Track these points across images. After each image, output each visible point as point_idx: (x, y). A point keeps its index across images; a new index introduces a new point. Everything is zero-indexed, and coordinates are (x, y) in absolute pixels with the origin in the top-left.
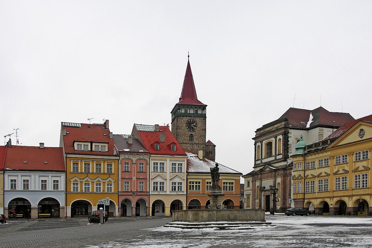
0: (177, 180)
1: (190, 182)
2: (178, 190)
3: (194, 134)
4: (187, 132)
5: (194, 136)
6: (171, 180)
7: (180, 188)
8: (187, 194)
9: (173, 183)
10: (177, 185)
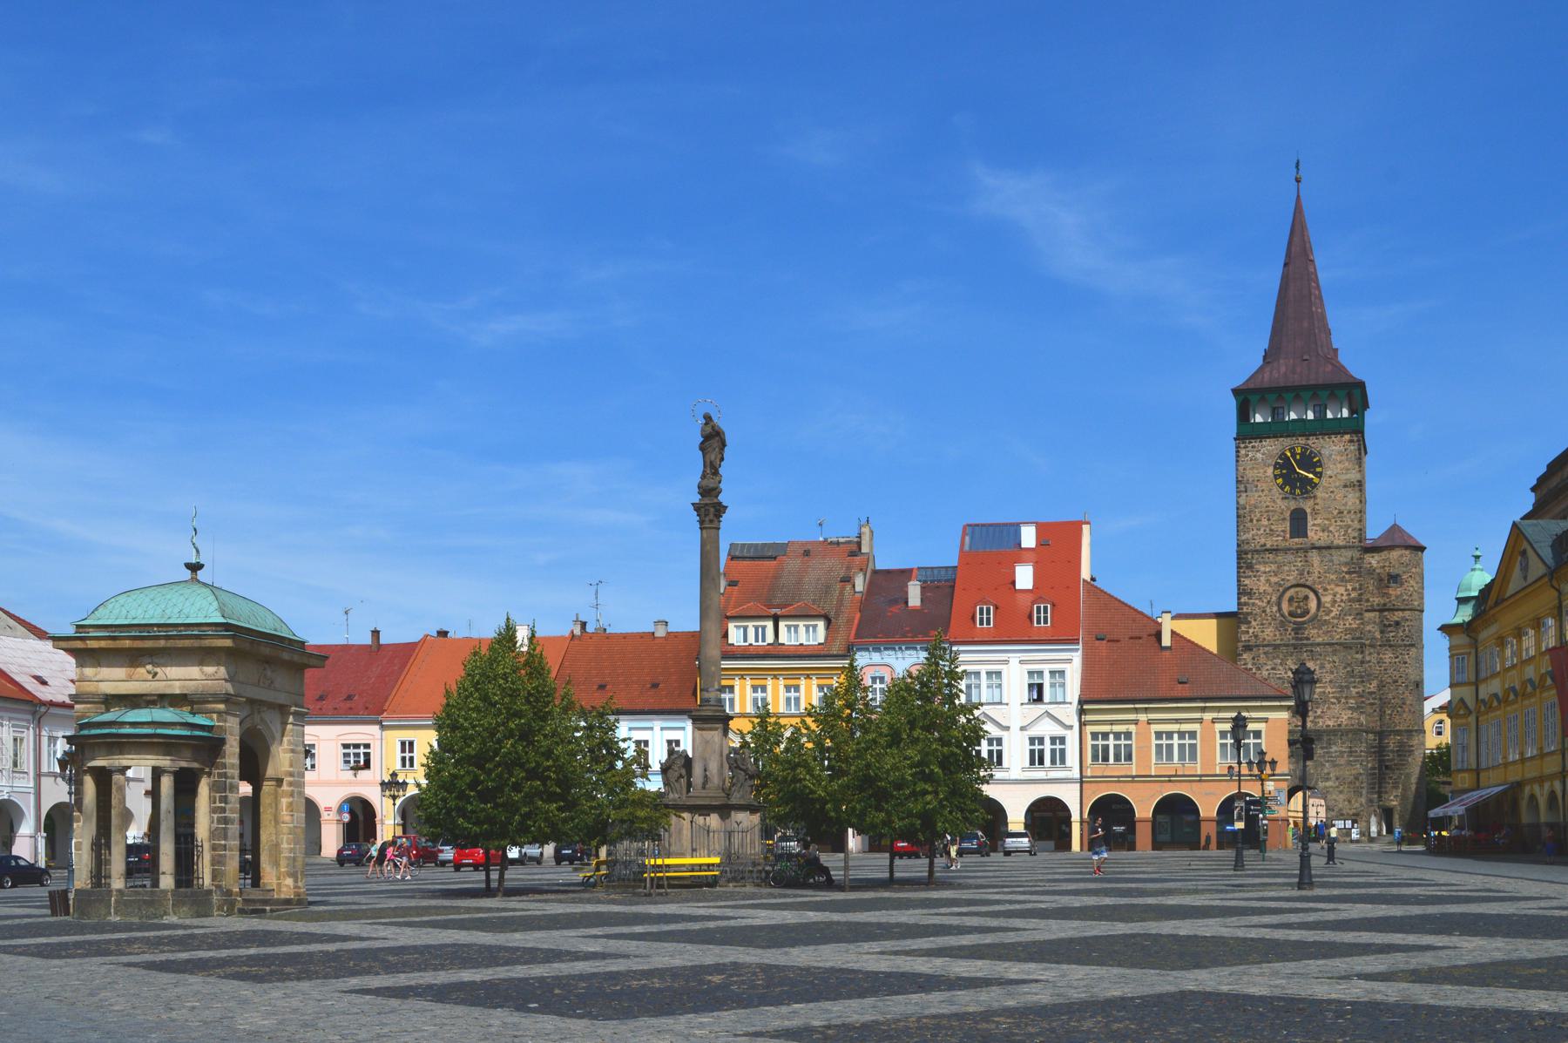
0: (1047, 729)
1: (1095, 736)
2: (1053, 762)
3: (1307, 506)
4: (1279, 501)
5: (1309, 517)
6: (1023, 729)
7: (1059, 758)
8: (1081, 778)
9: (1032, 740)
10: (1047, 747)
